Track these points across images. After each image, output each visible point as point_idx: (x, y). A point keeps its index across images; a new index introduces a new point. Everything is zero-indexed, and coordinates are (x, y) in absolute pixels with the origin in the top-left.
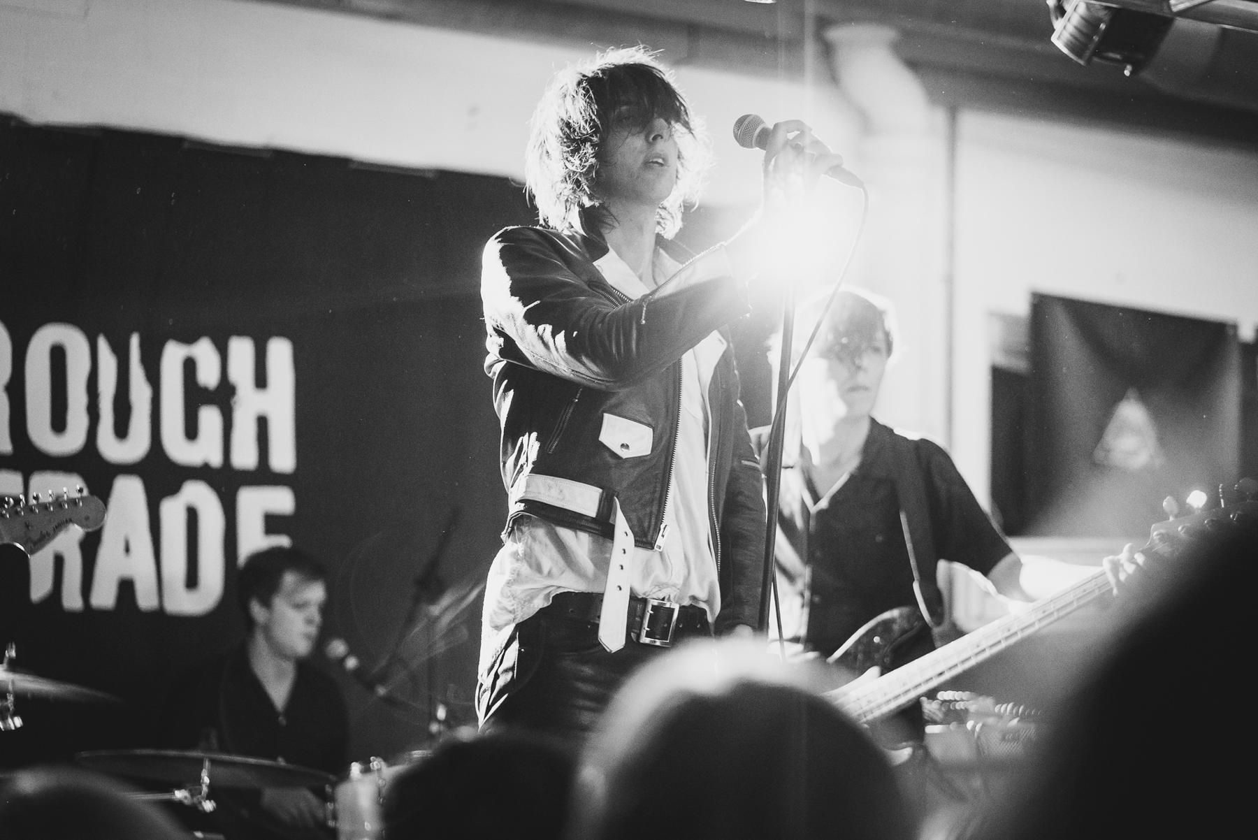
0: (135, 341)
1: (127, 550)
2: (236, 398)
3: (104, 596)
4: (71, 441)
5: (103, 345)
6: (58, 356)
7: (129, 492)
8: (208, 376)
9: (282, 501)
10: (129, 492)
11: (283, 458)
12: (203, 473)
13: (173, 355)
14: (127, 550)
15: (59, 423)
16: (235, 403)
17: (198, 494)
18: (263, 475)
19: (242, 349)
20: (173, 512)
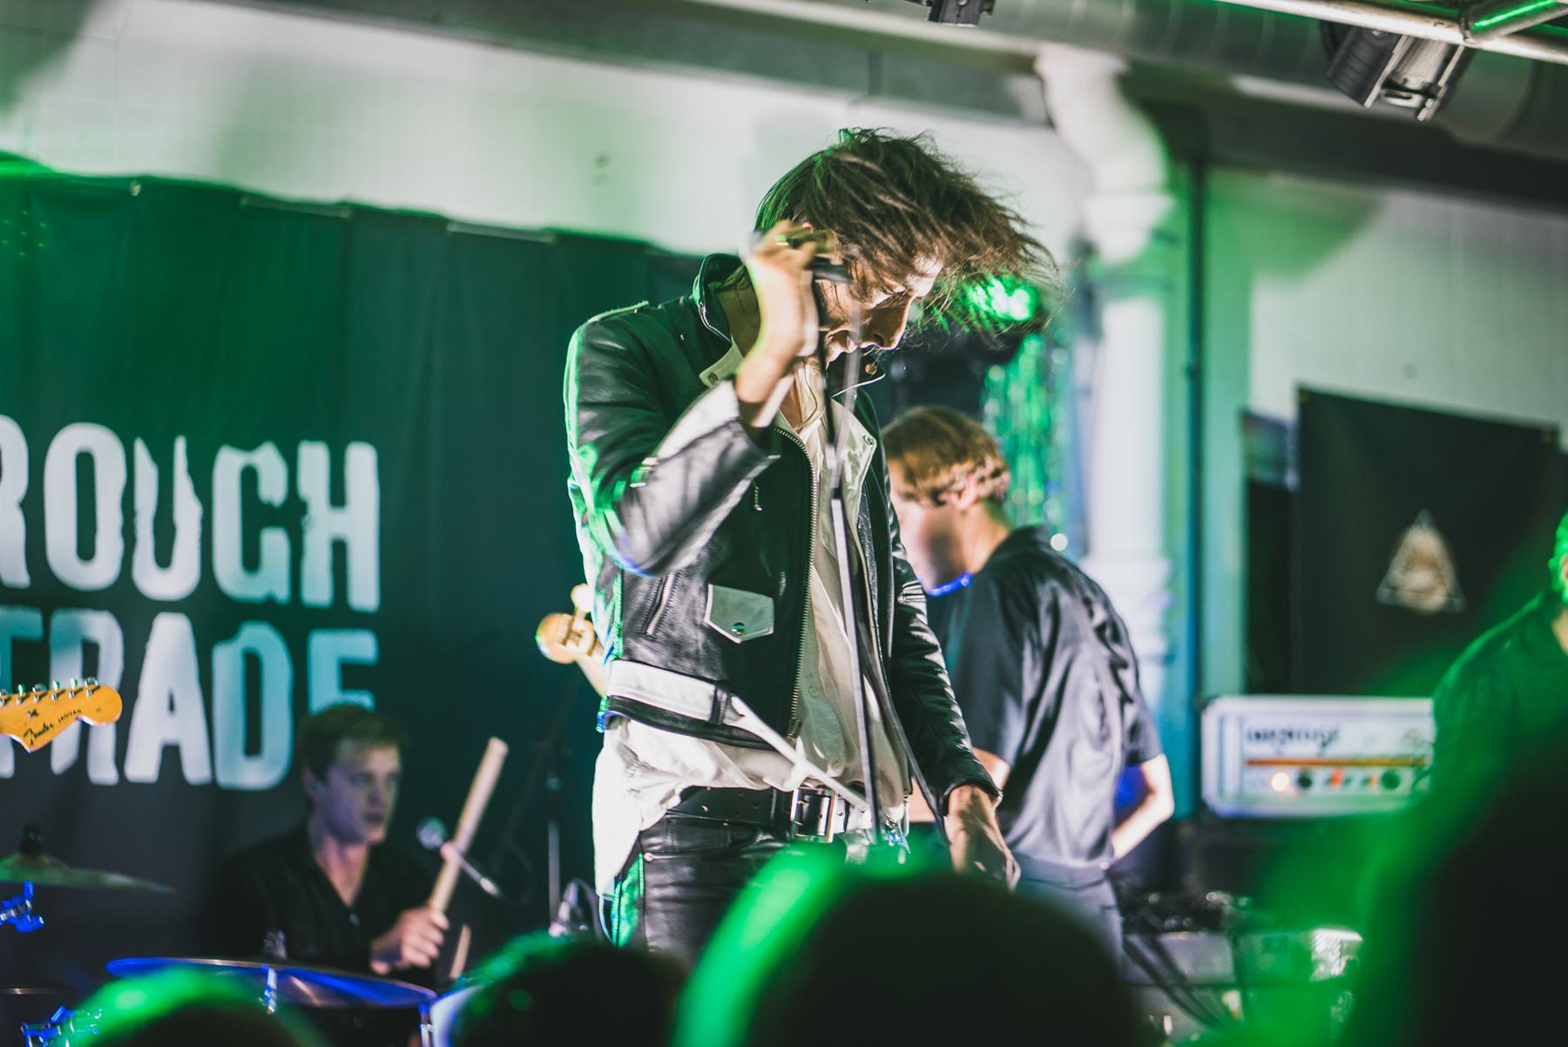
0: (180, 446)
1: (172, 707)
2: (307, 518)
3: (144, 766)
4: (101, 572)
5: (140, 449)
6: (85, 464)
8: (273, 489)
9: (363, 646)
11: (365, 592)
12: (265, 611)
13: (229, 464)
14: (172, 707)
15: (86, 550)
16: (306, 524)
17: (260, 637)
18: (340, 615)
19: (314, 457)
20: (227, 660)
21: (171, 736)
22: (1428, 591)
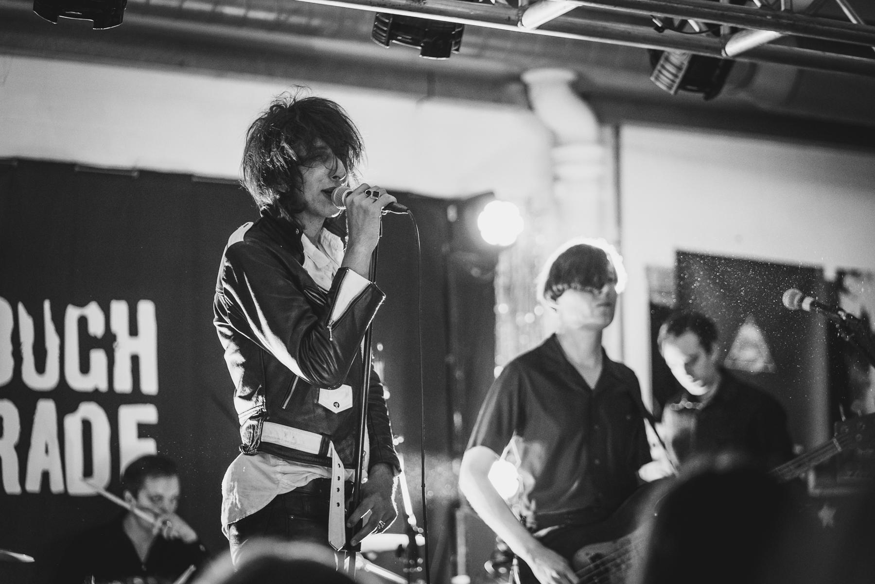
0: (47, 305)
1: (47, 451)
2: (115, 344)
5: (21, 308)
7: (46, 410)
8: (96, 328)
9: (149, 414)
10: (46, 410)
11: (150, 384)
12: (94, 396)
13: (72, 314)
14: (47, 451)
16: (116, 347)
17: (91, 411)
18: (136, 397)
19: (119, 309)
21: (46, 467)
22: (754, 361)
